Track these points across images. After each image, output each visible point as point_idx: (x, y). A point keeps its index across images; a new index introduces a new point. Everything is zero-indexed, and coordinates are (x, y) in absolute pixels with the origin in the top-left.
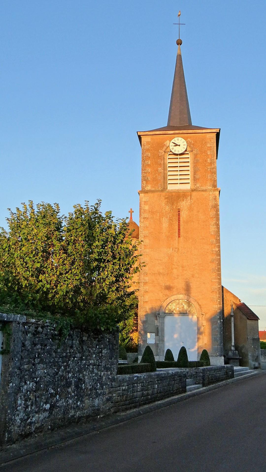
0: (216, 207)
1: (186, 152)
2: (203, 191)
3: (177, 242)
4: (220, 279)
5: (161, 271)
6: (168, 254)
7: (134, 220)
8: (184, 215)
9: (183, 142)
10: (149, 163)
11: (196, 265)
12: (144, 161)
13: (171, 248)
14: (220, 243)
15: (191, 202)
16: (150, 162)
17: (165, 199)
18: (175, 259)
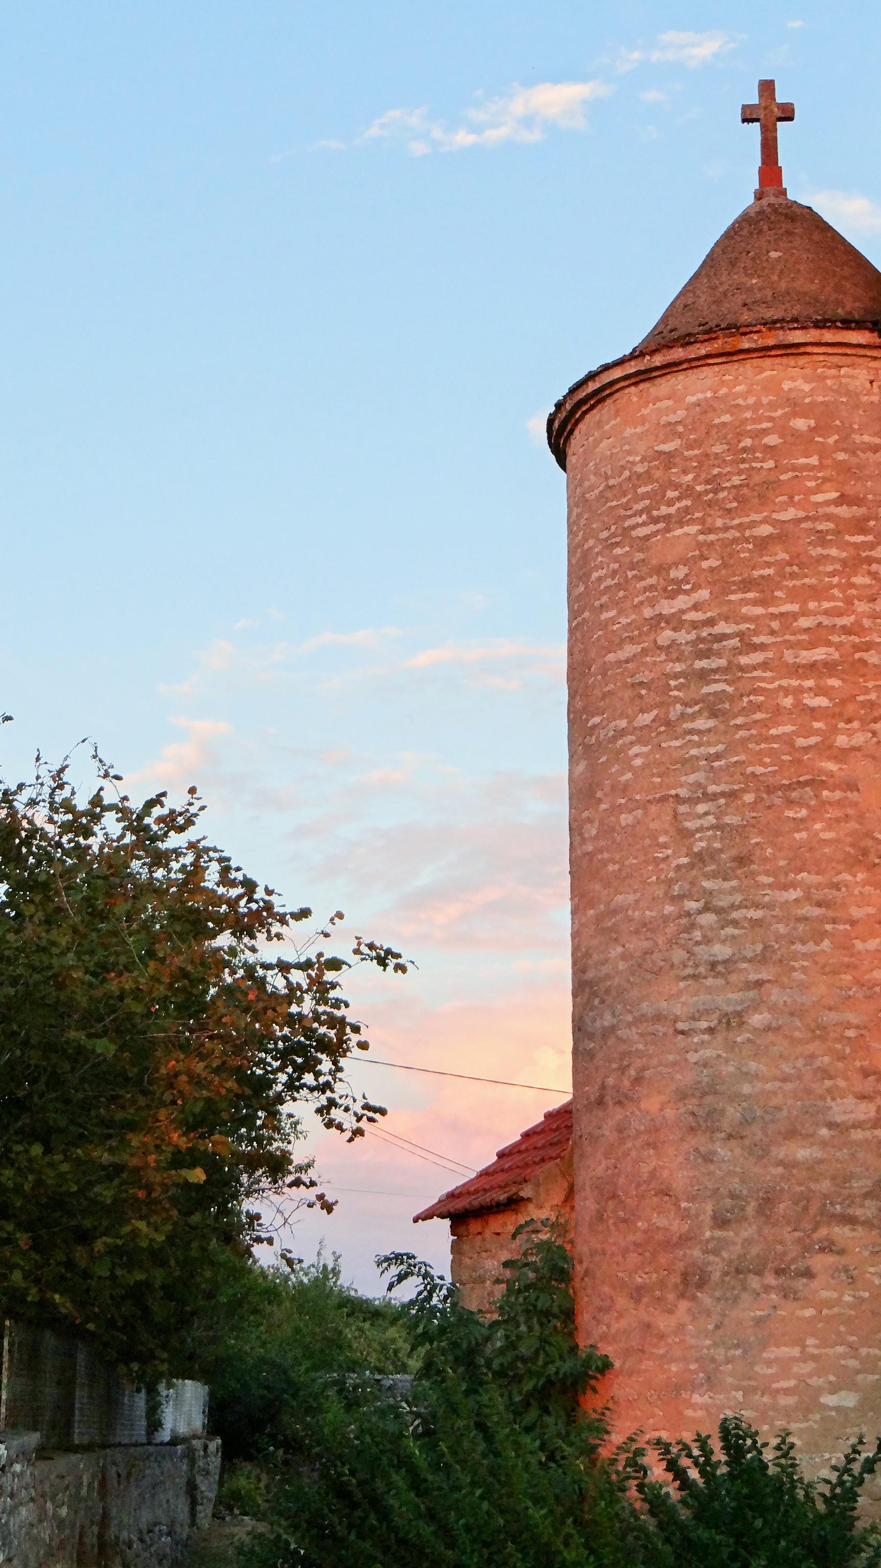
7: (799, 189)
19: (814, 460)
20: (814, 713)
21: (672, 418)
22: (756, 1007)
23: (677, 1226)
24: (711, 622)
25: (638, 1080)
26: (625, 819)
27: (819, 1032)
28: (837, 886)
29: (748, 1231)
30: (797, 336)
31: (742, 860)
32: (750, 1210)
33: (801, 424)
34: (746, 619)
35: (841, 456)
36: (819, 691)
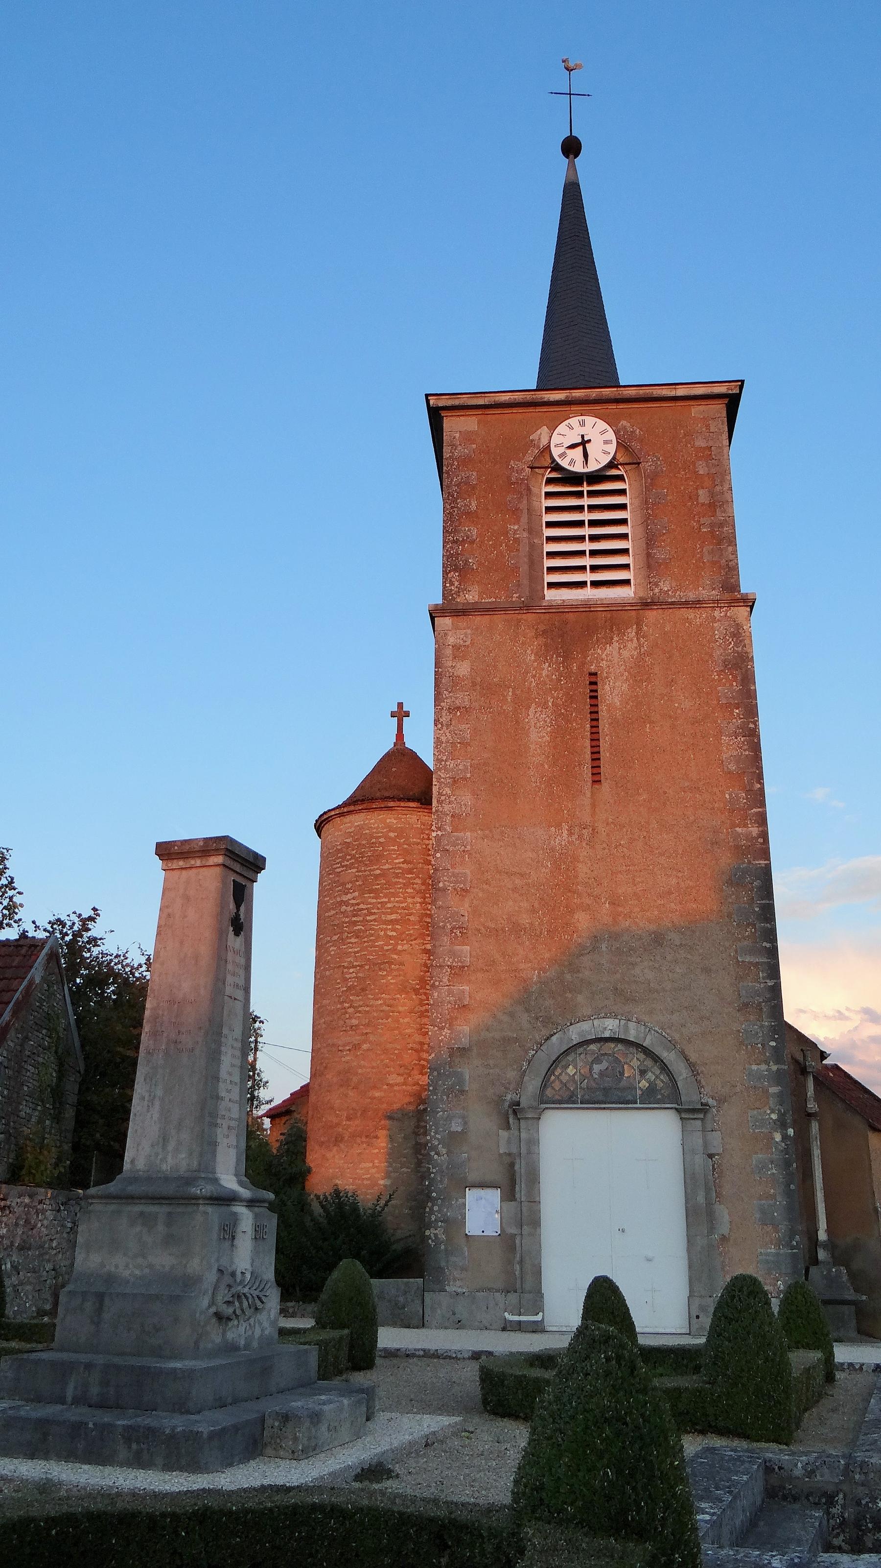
0: (741, 667)
1: (614, 472)
2: (686, 605)
3: (587, 801)
5: (525, 920)
6: (553, 849)
7: (410, 743)
8: (613, 693)
9: (603, 432)
10: (474, 506)
11: (670, 893)
12: (455, 501)
13: (565, 826)
14: (763, 804)
15: (640, 646)
18: (583, 870)
19: (396, 848)
20: (391, 937)
21: (350, 830)
22: (365, 1042)
23: (335, 1120)
24: (358, 904)
25: (326, 1068)
26: (328, 973)
27: (385, 1051)
28: (395, 999)
29: (357, 1122)
30: (391, 804)
31: (363, 990)
32: (359, 1115)
33: (392, 835)
34: (370, 904)
35: (405, 846)
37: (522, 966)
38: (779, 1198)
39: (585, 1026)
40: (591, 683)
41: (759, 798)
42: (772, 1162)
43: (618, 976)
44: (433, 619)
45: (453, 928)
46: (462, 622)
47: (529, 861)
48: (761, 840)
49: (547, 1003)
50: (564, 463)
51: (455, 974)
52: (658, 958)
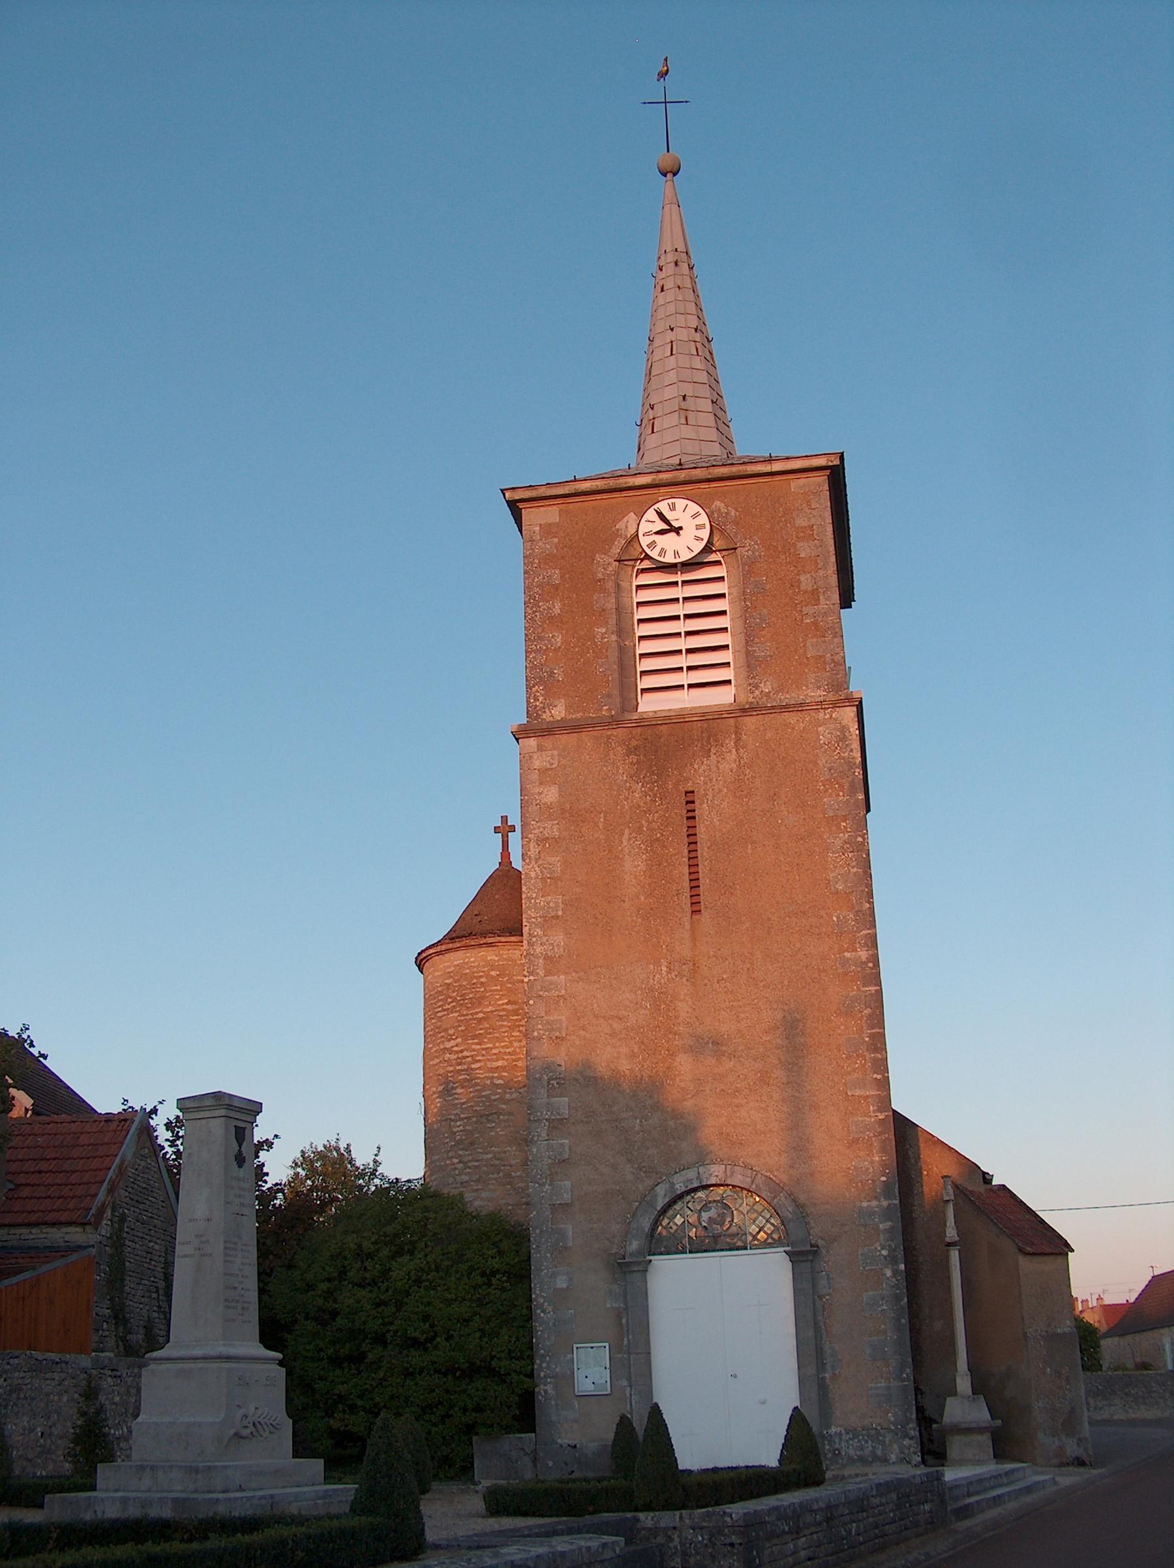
3: (687, 935)
4: (884, 1084)
6: (652, 990)
10: (557, 610)
14: (873, 925)
16: (558, 606)
17: (629, 753)
24: (462, 1051)
31: (472, 1144)
33: (493, 973)
36: (499, 1078)
37: (624, 1115)
38: (889, 1334)
39: (691, 1174)
40: (688, 802)
41: (869, 919)
42: (883, 1299)
43: (723, 1119)
44: (517, 740)
45: (550, 1080)
46: (548, 742)
47: (626, 1002)
48: (871, 965)
49: (650, 1152)
50: (654, 554)
51: (554, 1127)
52: (764, 1098)
